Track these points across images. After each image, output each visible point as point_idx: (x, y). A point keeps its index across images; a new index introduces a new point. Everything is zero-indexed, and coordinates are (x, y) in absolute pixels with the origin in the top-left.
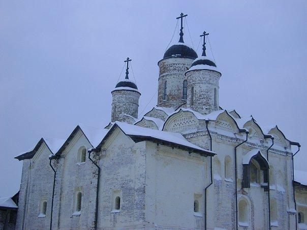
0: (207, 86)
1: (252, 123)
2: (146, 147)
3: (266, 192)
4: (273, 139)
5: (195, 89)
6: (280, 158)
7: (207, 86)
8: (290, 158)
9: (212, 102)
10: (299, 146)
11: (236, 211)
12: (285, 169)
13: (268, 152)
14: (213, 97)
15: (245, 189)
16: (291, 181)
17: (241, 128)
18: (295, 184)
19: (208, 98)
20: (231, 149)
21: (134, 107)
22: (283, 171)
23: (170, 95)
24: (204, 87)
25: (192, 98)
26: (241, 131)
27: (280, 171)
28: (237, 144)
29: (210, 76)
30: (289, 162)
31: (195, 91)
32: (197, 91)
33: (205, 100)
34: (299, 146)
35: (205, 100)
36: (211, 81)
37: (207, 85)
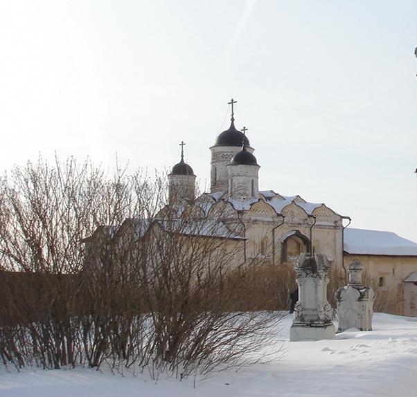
4: (315, 218)
6: (328, 233)
8: (341, 231)
12: (335, 241)
14: (250, 188)
16: (341, 251)
17: (279, 213)
18: (345, 254)
22: (332, 243)
23: (220, 180)
24: (241, 179)
25: (232, 188)
26: (278, 215)
27: (328, 243)
30: (339, 234)
34: (349, 218)
36: (248, 174)
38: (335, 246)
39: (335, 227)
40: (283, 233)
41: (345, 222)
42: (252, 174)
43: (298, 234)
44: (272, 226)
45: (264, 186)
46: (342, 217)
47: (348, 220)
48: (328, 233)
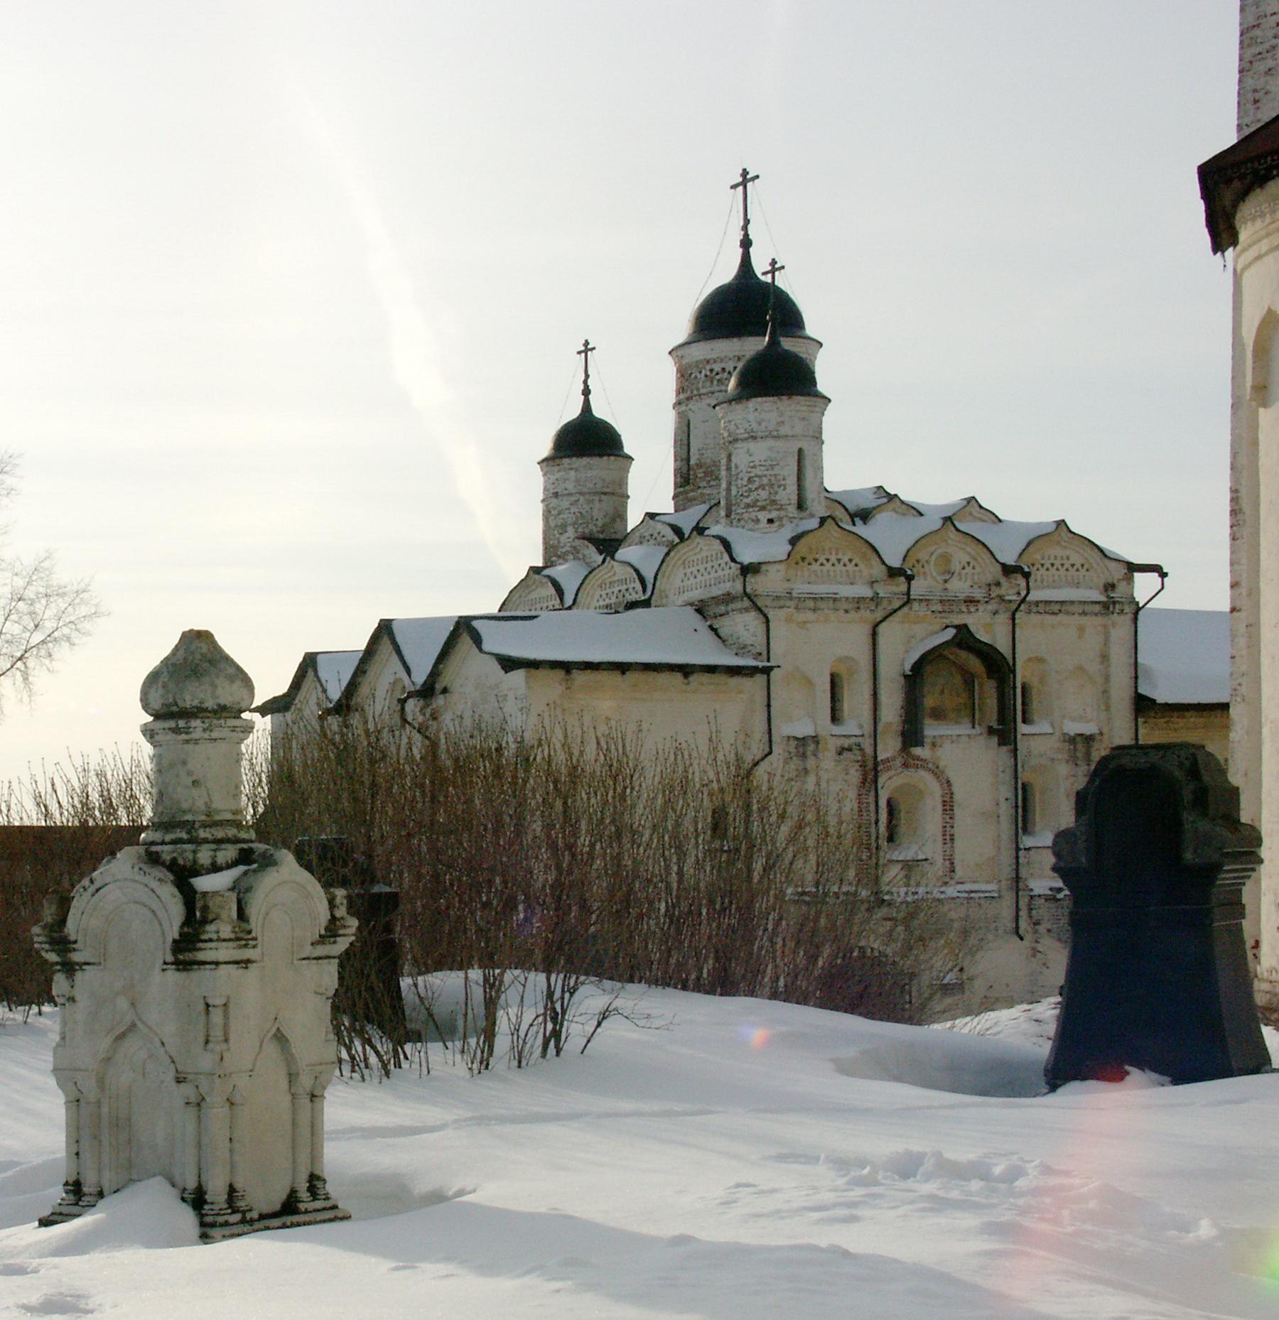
0: (770, 449)
1: (952, 534)
2: (529, 688)
3: (1004, 748)
5: (733, 458)
6: (1081, 629)
7: (770, 449)
9: (788, 494)
10: (1164, 575)
11: (873, 820)
12: (1105, 657)
13: (1013, 619)
15: (917, 751)
16: (1131, 692)
19: (775, 485)
20: (863, 632)
21: (608, 504)
22: (1094, 667)
24: (760, 451)
25: (729, 484)
26: (893, 573)
27: (1080, 668)
28: (879, 615)
29: (782, 415)
31: (737, 467)
32: (742, 467)
33: (764, 494)
34: (1164, 575)
35: (764, 494)
36: (784, 430)
37: (771, 442)
38: (1107, 678)
39: (1108, 606)
40: (906, 641)
41: (1144, 586)
42: (799, 428)
43: (964, 639)
44: (867, 614)
45: (845, 469)
46: (1133, 568)
47: (1154, 576)
48: (1081, 629)
